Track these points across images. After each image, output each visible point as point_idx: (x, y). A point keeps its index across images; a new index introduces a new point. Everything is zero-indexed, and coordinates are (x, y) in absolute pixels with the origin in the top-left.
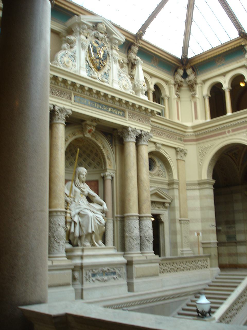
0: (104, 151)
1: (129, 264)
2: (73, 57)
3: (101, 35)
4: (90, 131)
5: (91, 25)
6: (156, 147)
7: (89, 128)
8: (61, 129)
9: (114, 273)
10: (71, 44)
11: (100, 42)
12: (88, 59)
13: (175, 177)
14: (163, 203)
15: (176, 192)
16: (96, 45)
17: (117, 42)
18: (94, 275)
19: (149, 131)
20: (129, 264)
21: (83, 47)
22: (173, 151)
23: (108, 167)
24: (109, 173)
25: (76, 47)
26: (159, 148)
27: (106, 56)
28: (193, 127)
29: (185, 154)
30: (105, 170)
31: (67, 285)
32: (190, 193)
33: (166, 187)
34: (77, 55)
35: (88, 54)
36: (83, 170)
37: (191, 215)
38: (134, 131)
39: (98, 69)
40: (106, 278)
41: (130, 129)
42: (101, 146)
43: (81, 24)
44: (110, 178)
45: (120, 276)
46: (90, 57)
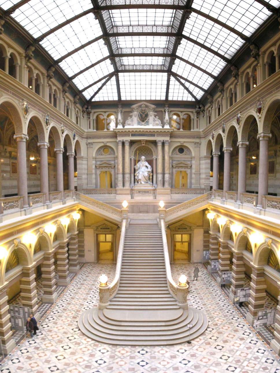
0: (152, 149)
1: (155, 190)
2: (132, 121)
3: (143, 109)
4: (143, 143)
5: (137, 107)
6: (181, 144)
7: (142, 143)
8: (127, 147)
9: (148, 192)
10: (131, 116)
11: (143, 112)
12: (139, 119)
13: (193, 155)
14: (187, 167)
15: (193, 162)
16: (142, 113)
17: (151, 108)
18: (139, 192)
19: (169, 140)
20: (155, 190)
21: (135, 116)
22: (193, 144)
23: (154, 155)
24: (154, 157)
25: (133, 117)
26: (183, 144)
27: (147, 115)
28: (203, 131)
29: (200, 144)
30: (153, 156)
31: (128, 194)
32: (202, 162)
33: (190, 159)
34: (134, 120)
35: (138, 118)
36: (143, 157)
37: (202, 171)
38: (160, 141)
39: (143, 121)
40: (144, 193)
41: (157, 141)
42: (151, 148)
43: (134, 108)
44: (155, 159)
45: (151, 193)
46: (139, 118)
